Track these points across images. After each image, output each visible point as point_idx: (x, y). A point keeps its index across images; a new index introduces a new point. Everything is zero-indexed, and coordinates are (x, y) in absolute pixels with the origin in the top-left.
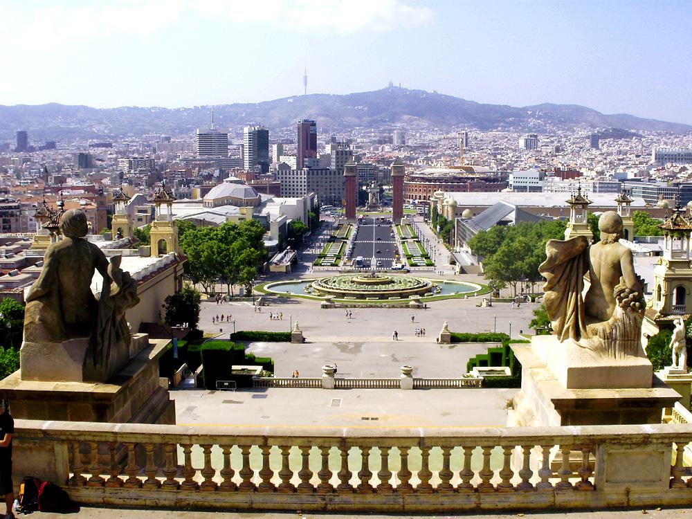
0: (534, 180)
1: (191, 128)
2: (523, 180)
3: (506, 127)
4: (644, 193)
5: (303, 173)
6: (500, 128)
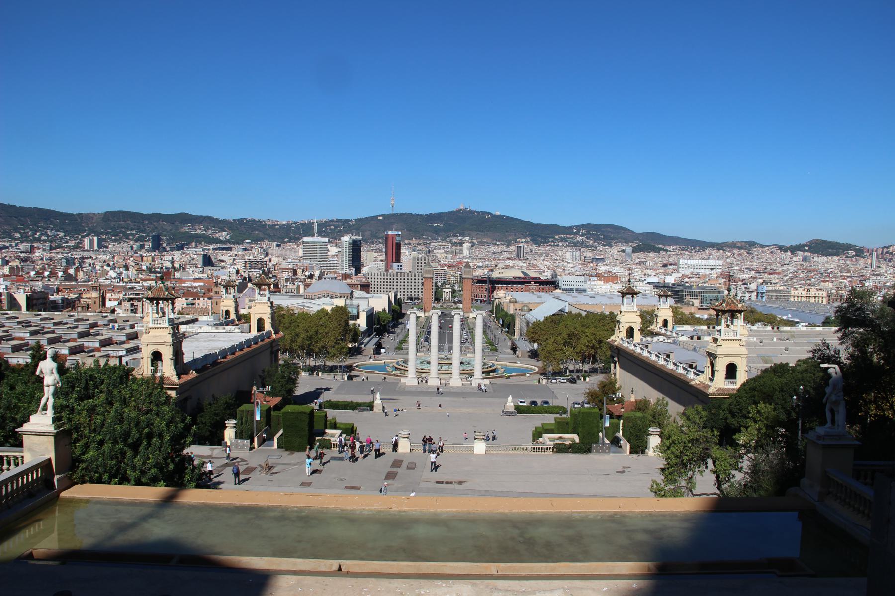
0: (580, 283)
1: (298, 237)
2: (571, 283)
3: (554, 243)
4: (678, 295)
5: (389, 275)
6: (550, 243)
